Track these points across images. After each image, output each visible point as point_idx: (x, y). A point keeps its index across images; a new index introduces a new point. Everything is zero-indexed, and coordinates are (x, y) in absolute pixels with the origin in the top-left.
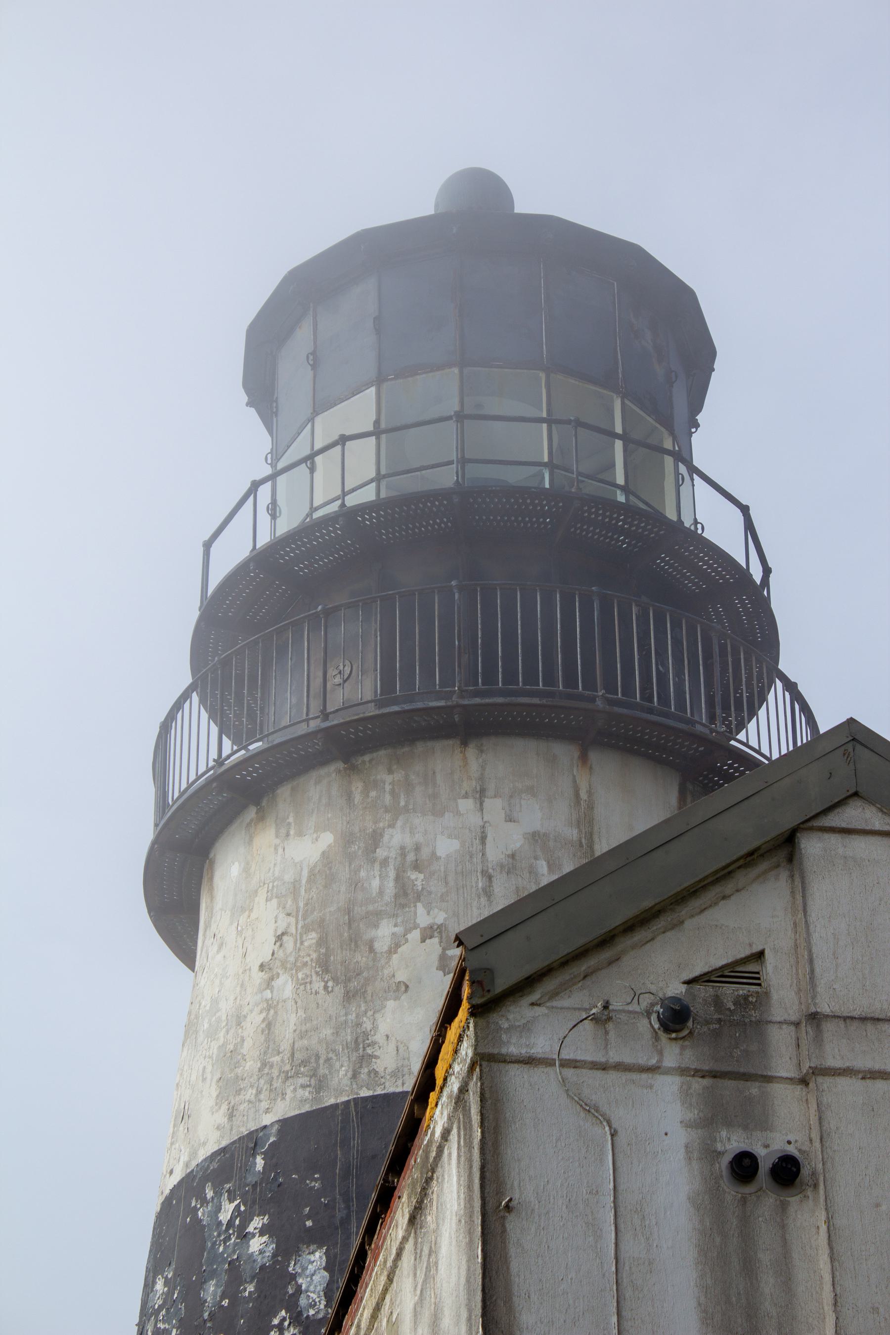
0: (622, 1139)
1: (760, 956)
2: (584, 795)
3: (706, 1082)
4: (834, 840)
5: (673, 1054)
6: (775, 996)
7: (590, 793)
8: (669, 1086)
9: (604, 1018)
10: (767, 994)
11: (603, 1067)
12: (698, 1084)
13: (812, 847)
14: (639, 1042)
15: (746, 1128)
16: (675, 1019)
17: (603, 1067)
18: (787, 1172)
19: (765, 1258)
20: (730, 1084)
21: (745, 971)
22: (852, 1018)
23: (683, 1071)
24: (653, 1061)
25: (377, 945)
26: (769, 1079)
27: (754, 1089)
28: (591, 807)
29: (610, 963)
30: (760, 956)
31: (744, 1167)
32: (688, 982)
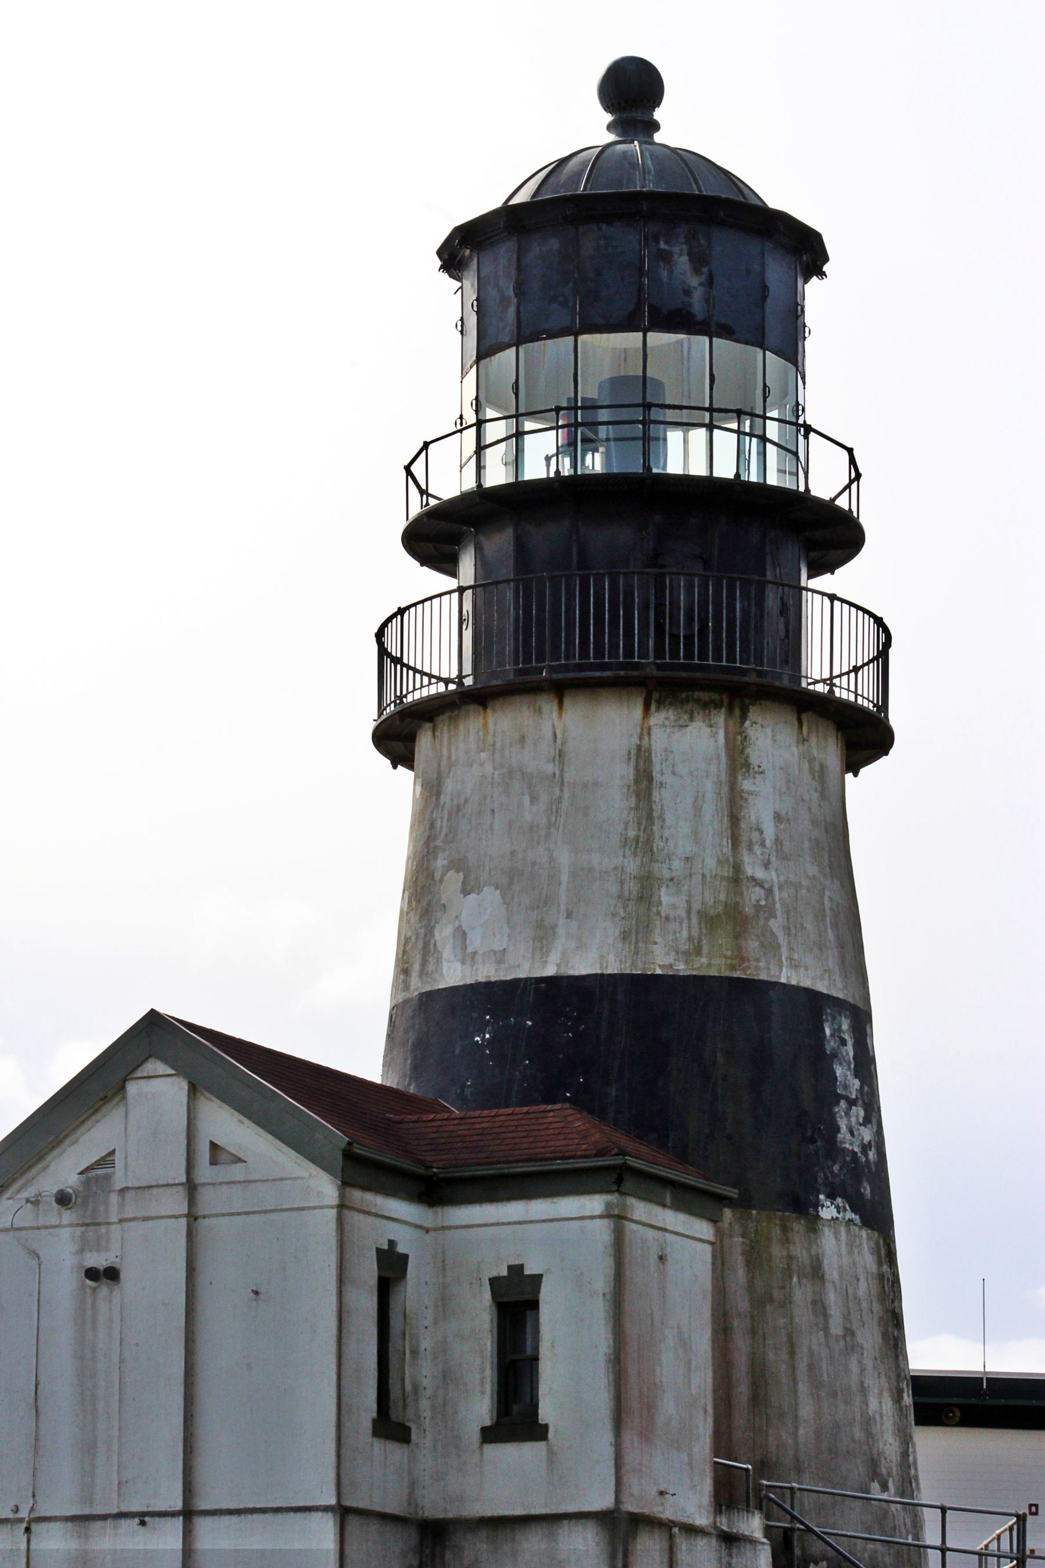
0: (43, 1267)
1: (114, 1150)
2: (559, 736)
3: (83, 1229)
4: (142, 1082)
5: (68, 1217)
6: (117, 1175)
7: (564, 731)
8: (65, 1233)
9: (35, 1202)
10: (114, 1173)
11: (38, 1228)
12: (79, 1230)
13: (133, 1088)
14: (52, 1214)
15: (98, 1251)
16: (63, 1199)
17: (38, 1228)
18: (112, 1274)
19: (102, 1319)
20: (92, 1228)
21: (107, 1160)
22: (139, 1188)
23: (71, 1225)
24: (58, 1223)
25: (436, 874)
26: (108, 1224)
27: (103, 1229)
28: (563, 744)
29: (44, 1169)
30: (114, 1150)
31: (92, 1274)
32: (81, 1173)
